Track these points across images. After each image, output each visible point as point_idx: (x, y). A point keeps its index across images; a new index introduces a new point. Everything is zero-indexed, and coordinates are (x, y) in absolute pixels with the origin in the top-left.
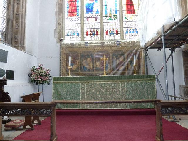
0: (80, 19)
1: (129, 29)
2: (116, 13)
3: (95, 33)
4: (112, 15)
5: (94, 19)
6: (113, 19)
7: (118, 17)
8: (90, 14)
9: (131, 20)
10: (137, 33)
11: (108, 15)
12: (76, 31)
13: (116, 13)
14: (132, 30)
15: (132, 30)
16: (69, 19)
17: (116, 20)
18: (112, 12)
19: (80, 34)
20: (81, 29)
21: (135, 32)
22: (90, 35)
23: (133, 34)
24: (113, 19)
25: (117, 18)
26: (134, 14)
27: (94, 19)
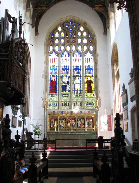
0: (58, 95)
1: (88, 102)
2: (81, 92)
3: (68, 104)
4: (78, 94)
5: (67, 96)
6: (79, 96)
7: (82, 95)
8: (64, 92)
9: (90, 96)
10: (93, 104)
11: (76, 93)
12: (55, 102)
13: (81, 92)
14: (90, 103)
15: (90, 103)
16: (51, 95)
17: (81, 97)
18: (78, 92)
19: (58, 104)
20: (59, 101)
21: (92, 104)
22: (65, 105)
23: (91, 105)
24: (79, 96)
25: (81, 95)
26: (92, 93)
27: (67, 96)
